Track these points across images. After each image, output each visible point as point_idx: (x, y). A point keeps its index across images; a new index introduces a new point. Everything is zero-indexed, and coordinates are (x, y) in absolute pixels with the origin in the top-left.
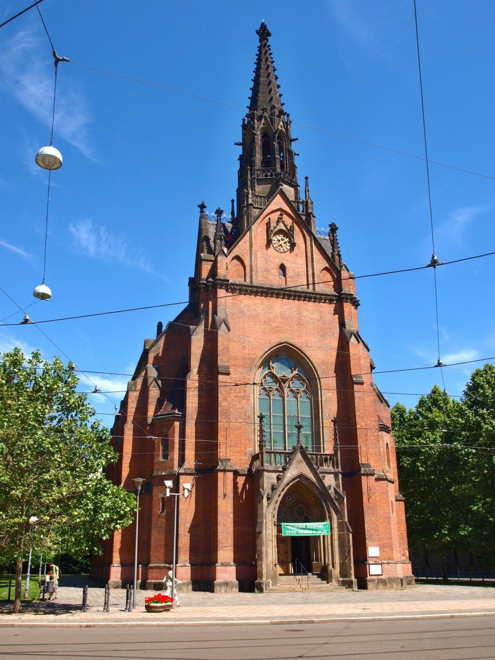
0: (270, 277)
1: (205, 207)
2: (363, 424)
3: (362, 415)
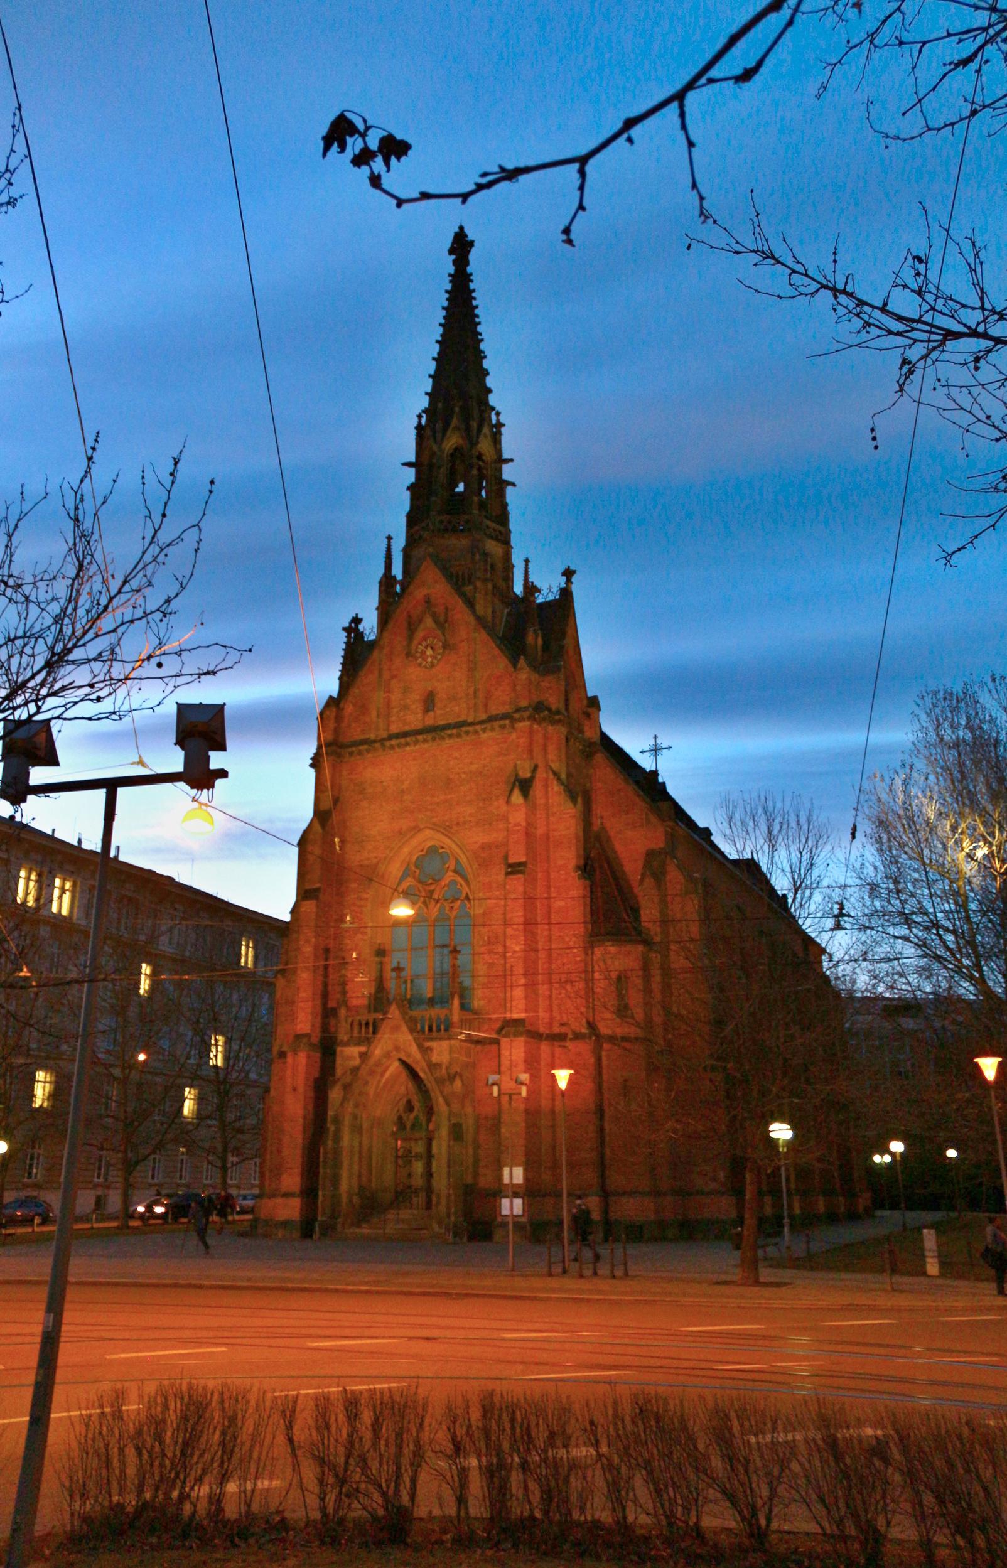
0: (410, 718)
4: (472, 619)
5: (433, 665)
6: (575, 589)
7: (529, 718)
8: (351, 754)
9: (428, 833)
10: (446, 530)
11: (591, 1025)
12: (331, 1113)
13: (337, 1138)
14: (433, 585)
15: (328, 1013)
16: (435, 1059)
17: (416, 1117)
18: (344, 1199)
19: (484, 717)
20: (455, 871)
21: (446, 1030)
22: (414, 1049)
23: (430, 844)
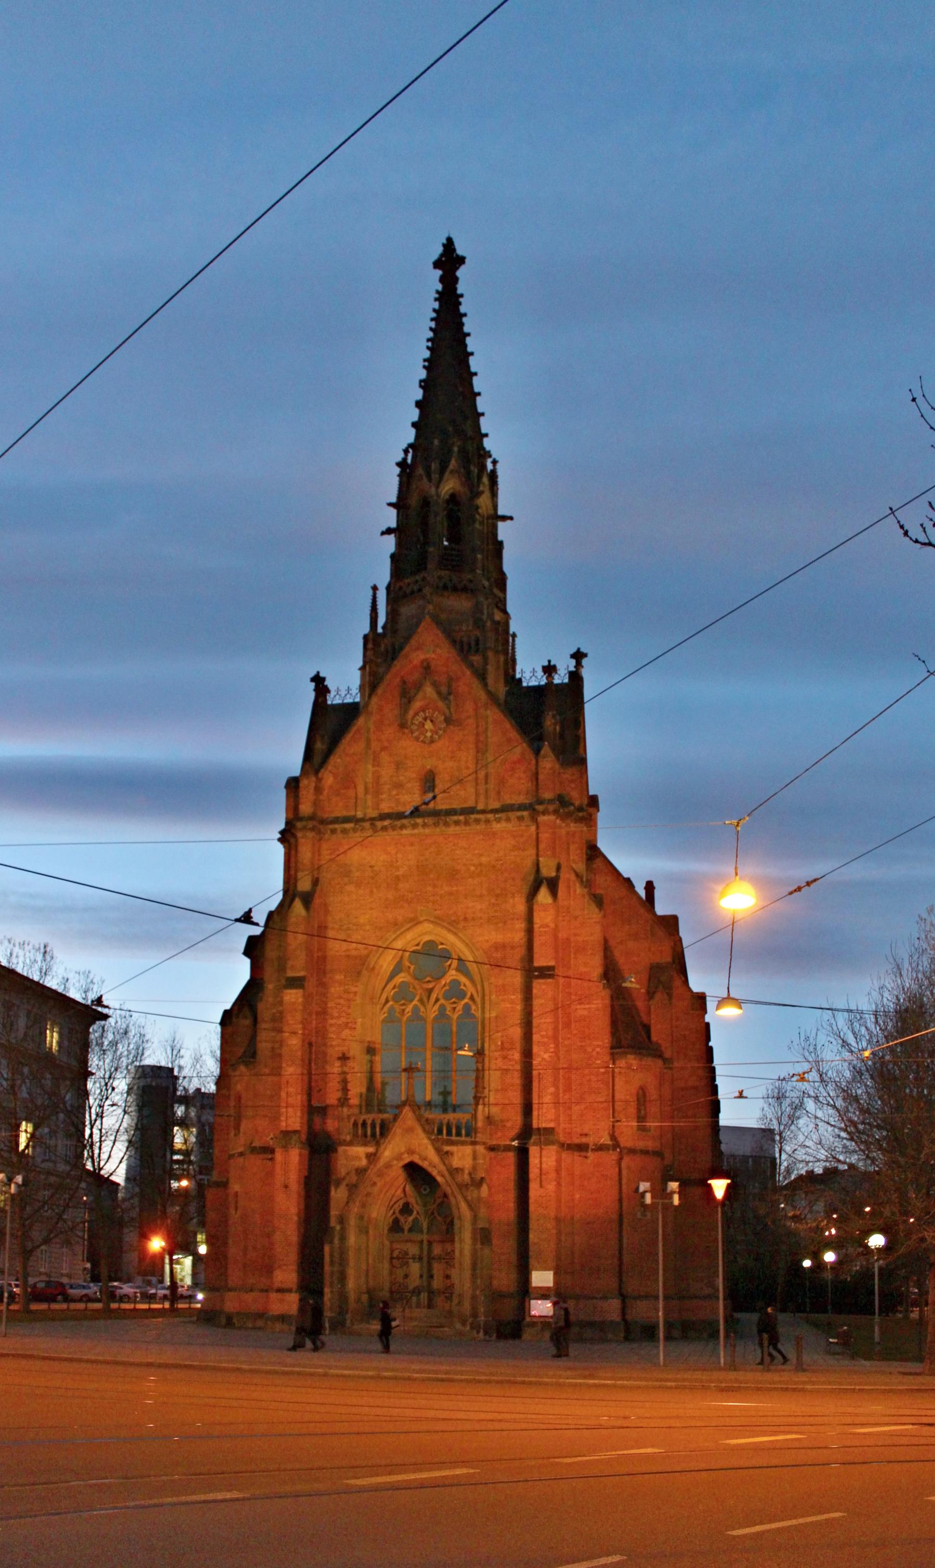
2: (546, 1056)
3: (546, 1040)
4: (483, 695)
5: (432, 741)
6: (585, 673)
7: (556, 812)
8: (333, 831)
9: (427, 926)
10: (445, 587)
11: (613, 1137)
12: (334, 1213)
13: (343, 1238)
14: (429, 648)
15: (315, 1110)
16: (456, 1162)
17: (416, 1221)
18: (352, 1296)
19: (496, 805)
20: (457, 970)
21: (468, 1134)
23: (427, 938)
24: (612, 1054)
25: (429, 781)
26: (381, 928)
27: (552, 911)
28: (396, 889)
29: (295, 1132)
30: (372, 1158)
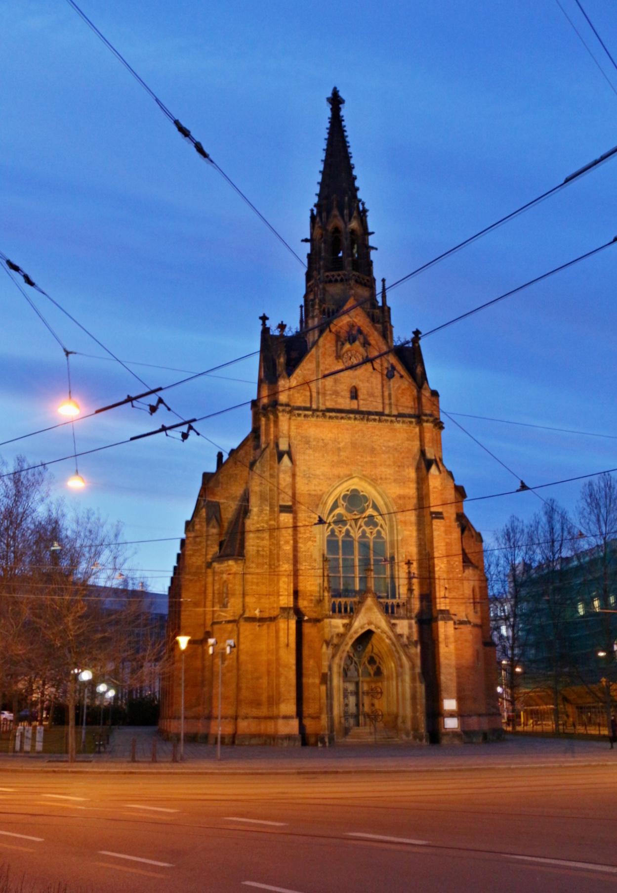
1: (267, 319)
2: (442, 566)
8: (299, 415)
16: (399, 630)
19: (395, 412)
22: (383, 624)
23: (353, 487)
24: (464, 567)
25: (354, 394)
26: (330, 479)
27: (439, 480)
28: (339, 456)
29: (290, 608)
30: (348, 627)
